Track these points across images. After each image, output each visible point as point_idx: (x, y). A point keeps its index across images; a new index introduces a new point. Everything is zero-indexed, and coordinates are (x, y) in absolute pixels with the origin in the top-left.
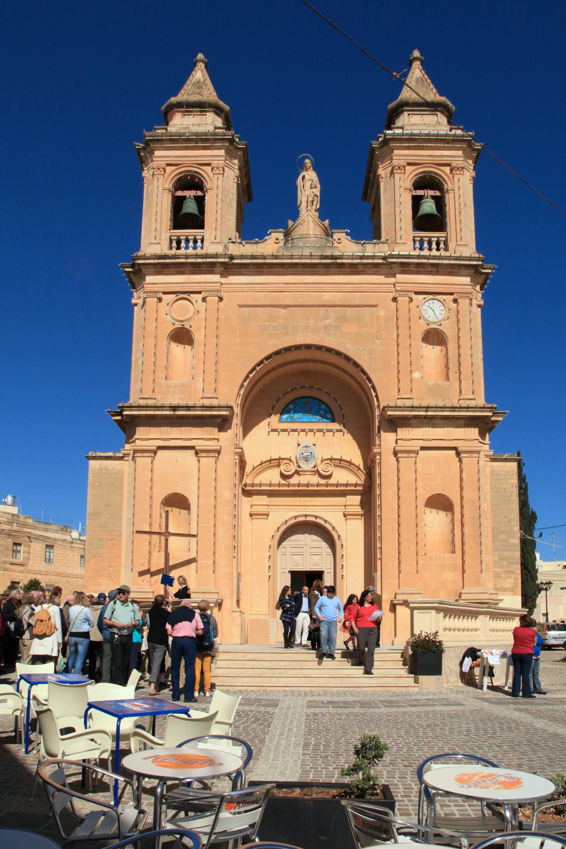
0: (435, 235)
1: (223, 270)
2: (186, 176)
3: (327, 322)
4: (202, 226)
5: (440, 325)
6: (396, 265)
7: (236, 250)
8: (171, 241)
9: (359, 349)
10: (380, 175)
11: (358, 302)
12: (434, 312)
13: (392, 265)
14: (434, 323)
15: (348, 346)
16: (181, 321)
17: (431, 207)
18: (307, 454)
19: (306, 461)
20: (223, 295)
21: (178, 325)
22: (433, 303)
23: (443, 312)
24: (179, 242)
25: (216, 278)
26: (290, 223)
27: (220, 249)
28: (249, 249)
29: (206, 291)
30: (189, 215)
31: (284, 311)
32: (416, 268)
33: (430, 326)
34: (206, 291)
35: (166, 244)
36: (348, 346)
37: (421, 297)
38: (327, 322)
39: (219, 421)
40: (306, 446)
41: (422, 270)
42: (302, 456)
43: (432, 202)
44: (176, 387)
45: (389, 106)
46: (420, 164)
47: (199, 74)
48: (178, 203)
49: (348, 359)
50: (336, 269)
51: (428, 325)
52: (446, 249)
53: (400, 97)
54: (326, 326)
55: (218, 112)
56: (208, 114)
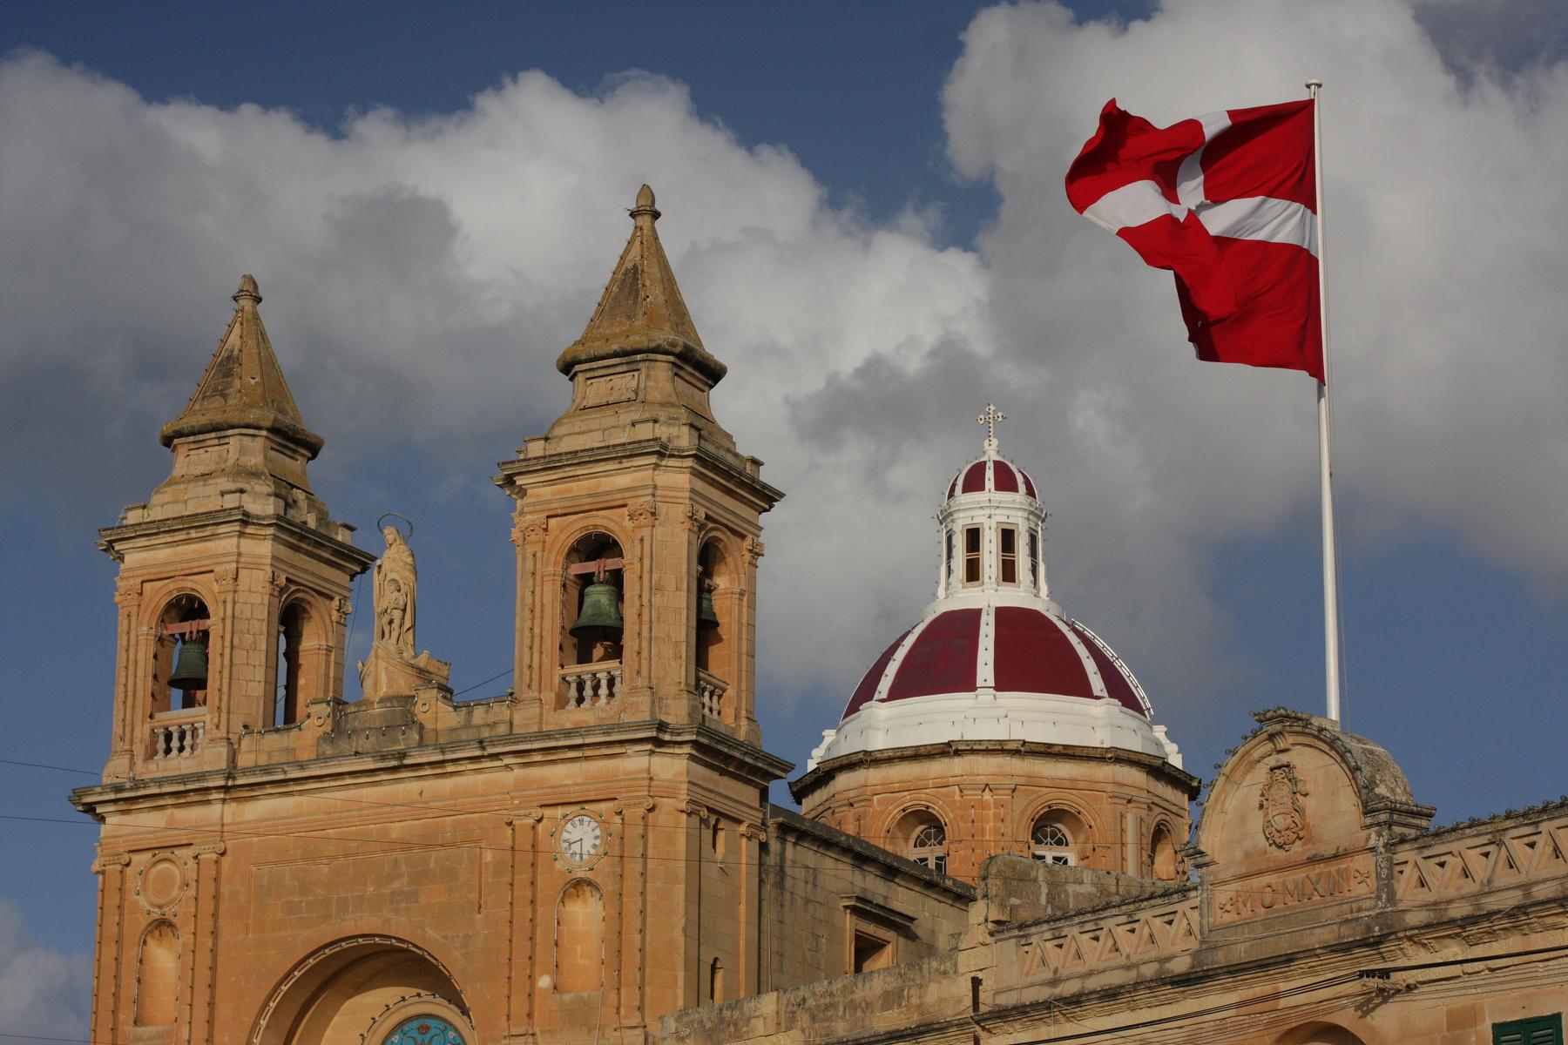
0: (601, 668)
2: (179, 599)
3: (396, 885)
9: (446, 938)
15: (430, 932)
16: (160, 907)
17: (597, 604)
20: (230, 844)
22: (581, 822)
25: (214, 812)
36: (430, 932)
37: (560, 811)
38: (396, 885)
43: (600, 593)
44: (150, 1039)
54: (393, 893)
56: (231, 440)
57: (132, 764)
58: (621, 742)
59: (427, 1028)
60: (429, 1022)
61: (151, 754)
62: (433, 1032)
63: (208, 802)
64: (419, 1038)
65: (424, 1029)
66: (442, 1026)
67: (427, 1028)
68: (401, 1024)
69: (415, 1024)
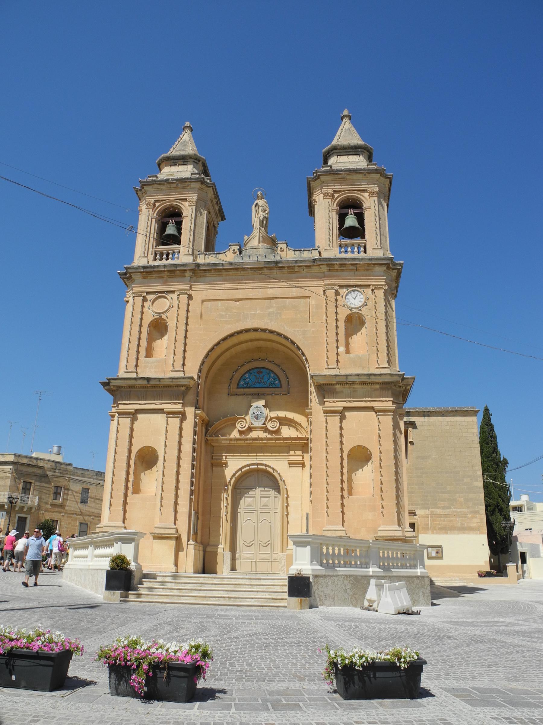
1: (191, 274)
2: (169, 208)
3: (270, 310)
4: (179, 243)
5: (361, 310)
6: (323, 266)
7: (201, 260)
8: (156, 254)
9: (295, 331)
10: (314, 200)
11: (295, 295)
12: (355, 300)
13: (321, 266)
14: (355, 308)
16: (159, 313)
18: (257, 413)
19: (257, 419)
21: (157, 316)
23: (362, 300)
24: (161, 255)
26: (246, 237)
27: (189, 260)
28: (211, 259)
29: (178, 291)
30: (169, 235)
31: (238, 303)
32: (340, 267)
33: (353, 311)
34: (178, 291)
35: (151, 257)
38: (270, 310)
39: (183, 389)
40: (257, 407)
41: (344, 268)
42: (254, 415)
45: (323, 151)
46: (344, 191)
47: (186, 136)
48: (162, 227)
49: (286, 338)
50: (278, 271)
51: (351, 310)
52: (365, 252)
53: (332, 143)
54: (269, 313)
55: (196, 161)
57: (148, 262)
58: (374, 264)
59: (262, 372)
60: (262, 370)
61: (155, 259)
62: (264, 374)
63: (184, 276)
64: (258, 376)
65: (260, 373)
66: (268, 371)
67: (262, 372)
68: (250, 370)
69: (256, 370)
